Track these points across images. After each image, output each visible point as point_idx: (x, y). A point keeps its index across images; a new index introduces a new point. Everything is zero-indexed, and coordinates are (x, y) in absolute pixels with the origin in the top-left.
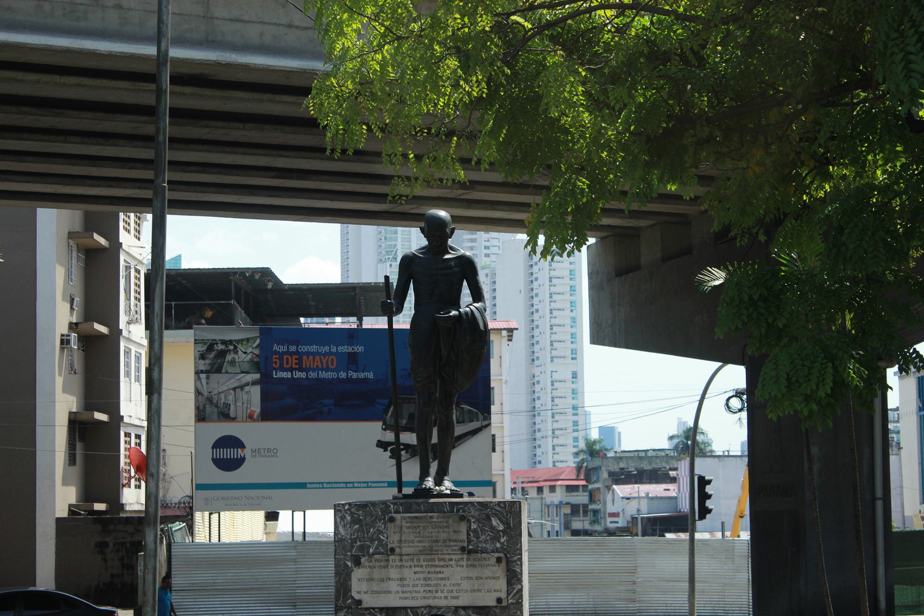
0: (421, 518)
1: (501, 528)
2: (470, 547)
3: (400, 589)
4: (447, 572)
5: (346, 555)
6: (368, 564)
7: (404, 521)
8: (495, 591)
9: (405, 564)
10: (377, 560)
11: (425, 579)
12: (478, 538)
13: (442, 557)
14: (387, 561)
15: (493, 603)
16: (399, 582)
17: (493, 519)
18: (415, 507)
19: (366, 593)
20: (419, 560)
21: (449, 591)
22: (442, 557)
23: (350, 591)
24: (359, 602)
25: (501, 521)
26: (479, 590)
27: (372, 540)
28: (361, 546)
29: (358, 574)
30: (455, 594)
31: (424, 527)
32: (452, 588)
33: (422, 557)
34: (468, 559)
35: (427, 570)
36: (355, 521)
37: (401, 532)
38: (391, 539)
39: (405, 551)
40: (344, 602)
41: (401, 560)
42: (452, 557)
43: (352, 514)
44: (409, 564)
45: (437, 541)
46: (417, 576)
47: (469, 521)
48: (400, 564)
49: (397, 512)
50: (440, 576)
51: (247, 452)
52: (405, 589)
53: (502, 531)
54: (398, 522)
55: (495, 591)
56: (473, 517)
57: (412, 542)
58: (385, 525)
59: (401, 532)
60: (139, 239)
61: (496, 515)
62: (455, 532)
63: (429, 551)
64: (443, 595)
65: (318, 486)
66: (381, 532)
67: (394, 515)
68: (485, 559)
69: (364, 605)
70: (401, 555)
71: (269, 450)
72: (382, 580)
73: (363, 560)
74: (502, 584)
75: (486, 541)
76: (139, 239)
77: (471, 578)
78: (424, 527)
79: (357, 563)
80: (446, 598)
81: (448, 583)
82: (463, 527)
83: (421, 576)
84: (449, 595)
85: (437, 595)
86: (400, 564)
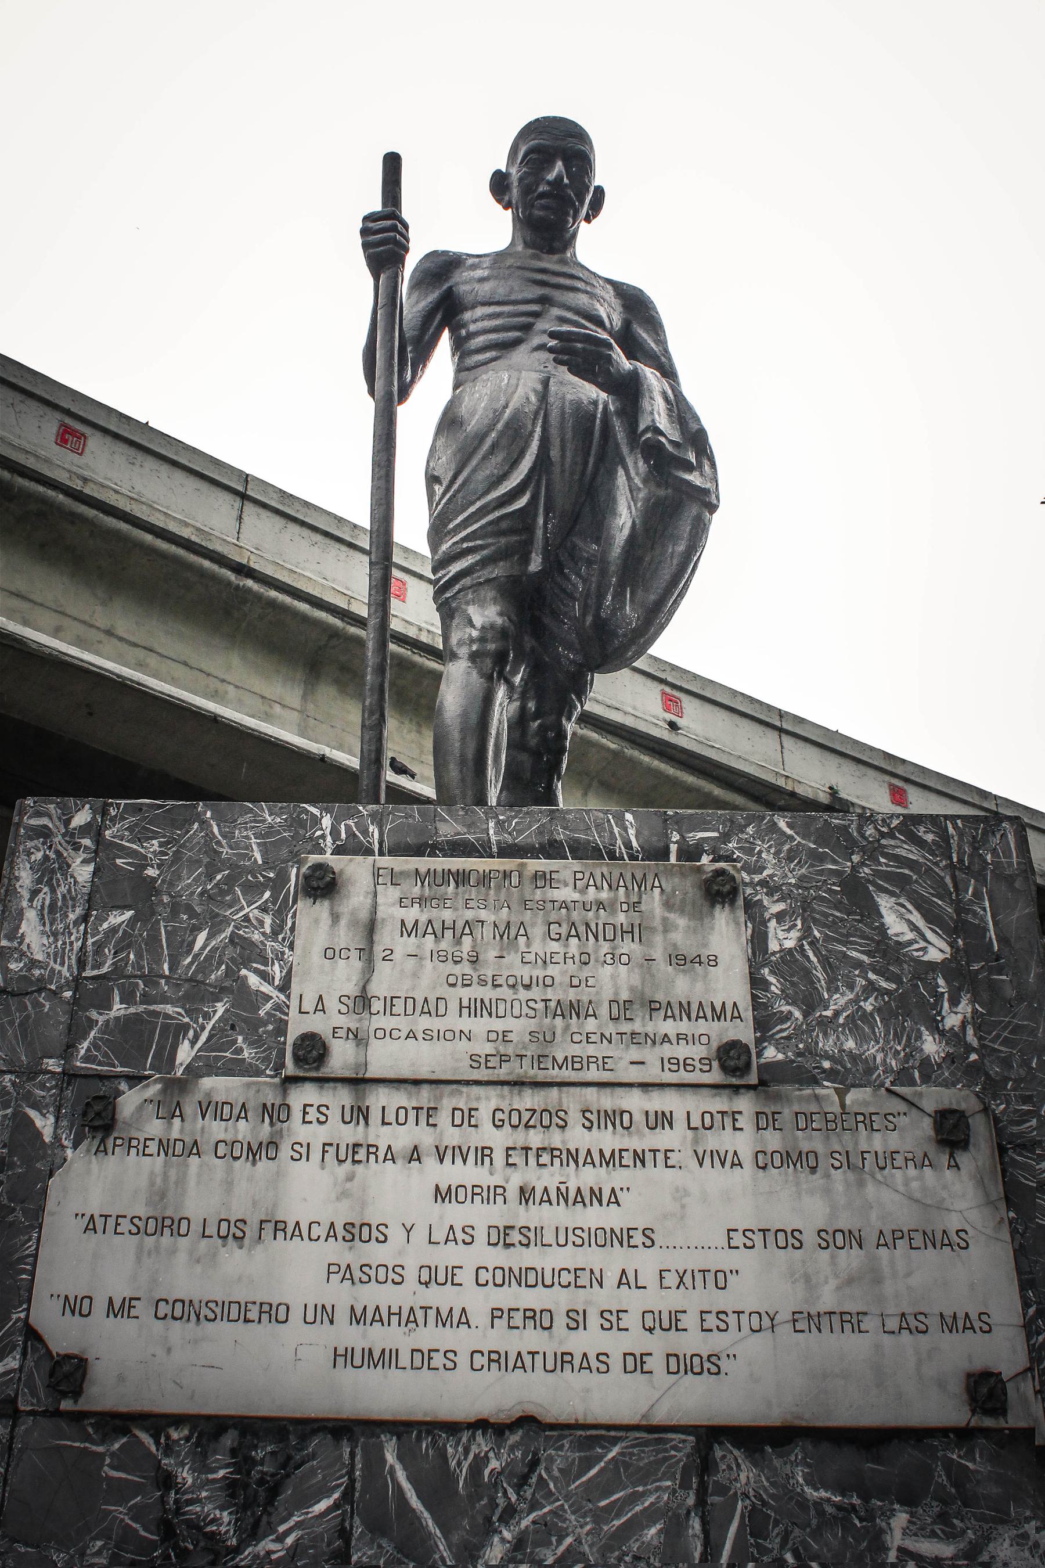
2: (771, 1053)
4: (643, 1196)
5: (33, 1072)
7: (389, 895)
9: (382, 1136)
11: (503, 1236)
12: (810, 1003)
13: (607, 1101)
14: (276, 1113)
15: (946, 1409)
17: (885, 903)
20: (468, 1118)
22: (607, 1101)
23: (26, 1295)
25: (931, 917)
27: (196, 994)
30: (692, 1342)
33: (488, 1101)
34: (764, 1121)
35: (516, 1180)
37: (367, 953)
38: (305, 989)
39: (383, 1058)
41: (360, 1114)
44: (402, 1137)
45: (574, 1009)
46: (457, 1214)
47: (752, 909)
48: (350, 1134)
50: (594, 1217)
52: (374, 1296)
54: (356, 900)
56: (771, 888)
57: (430, 1008)
59: (367, 953)
61: (900, 885)
62: (680, 960)
64: (615, 1344)
66: (248, 953)
72: (234, 1232)
73: (130, 1101)
75: (858, 1022)
77: (792, 1239)
78: (508, 935)
80: (637, 1363)
81: (645, 1263)
83: (482, 1216)
84: (658, 1344)
85: (579, 1343)
86: (350, 1134)
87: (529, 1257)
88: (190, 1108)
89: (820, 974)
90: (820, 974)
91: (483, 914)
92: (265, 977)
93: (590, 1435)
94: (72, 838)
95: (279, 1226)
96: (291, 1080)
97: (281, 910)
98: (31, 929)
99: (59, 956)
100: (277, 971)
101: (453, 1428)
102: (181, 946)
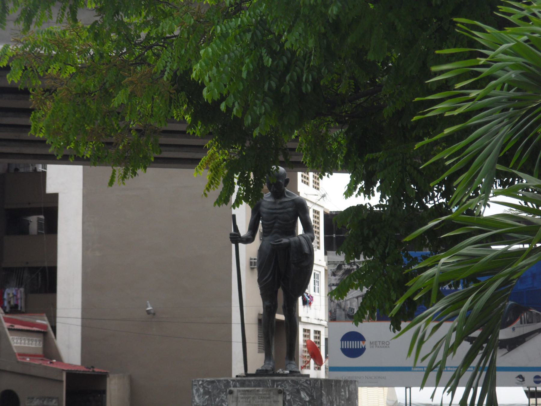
0: (251, 391)
1: (307, 399)
7: (239, 393)
17: (302, 393)
18: (247, 383)
25: (307, 394)
31: (253, 398)
36: (206, 393)
43: (204, 388)
47: (284, 394)
49: (235, 386)
51: (367, 344)
53: (309, 402)
54: (235, 394)
56: (287, 390)
58: (227, 395)
60: (318, 189)
61: (304, 390)
65: (420, 369)
67: (232, 388)
71: (383, 343)
76: (318, 189)
78: (253, 398)
82: (280, 398)
89: (292, 403)
90: (292, 403)
94: (200, 385)
97: (227, 395)
99: (200, 402)
102: (215, 400)
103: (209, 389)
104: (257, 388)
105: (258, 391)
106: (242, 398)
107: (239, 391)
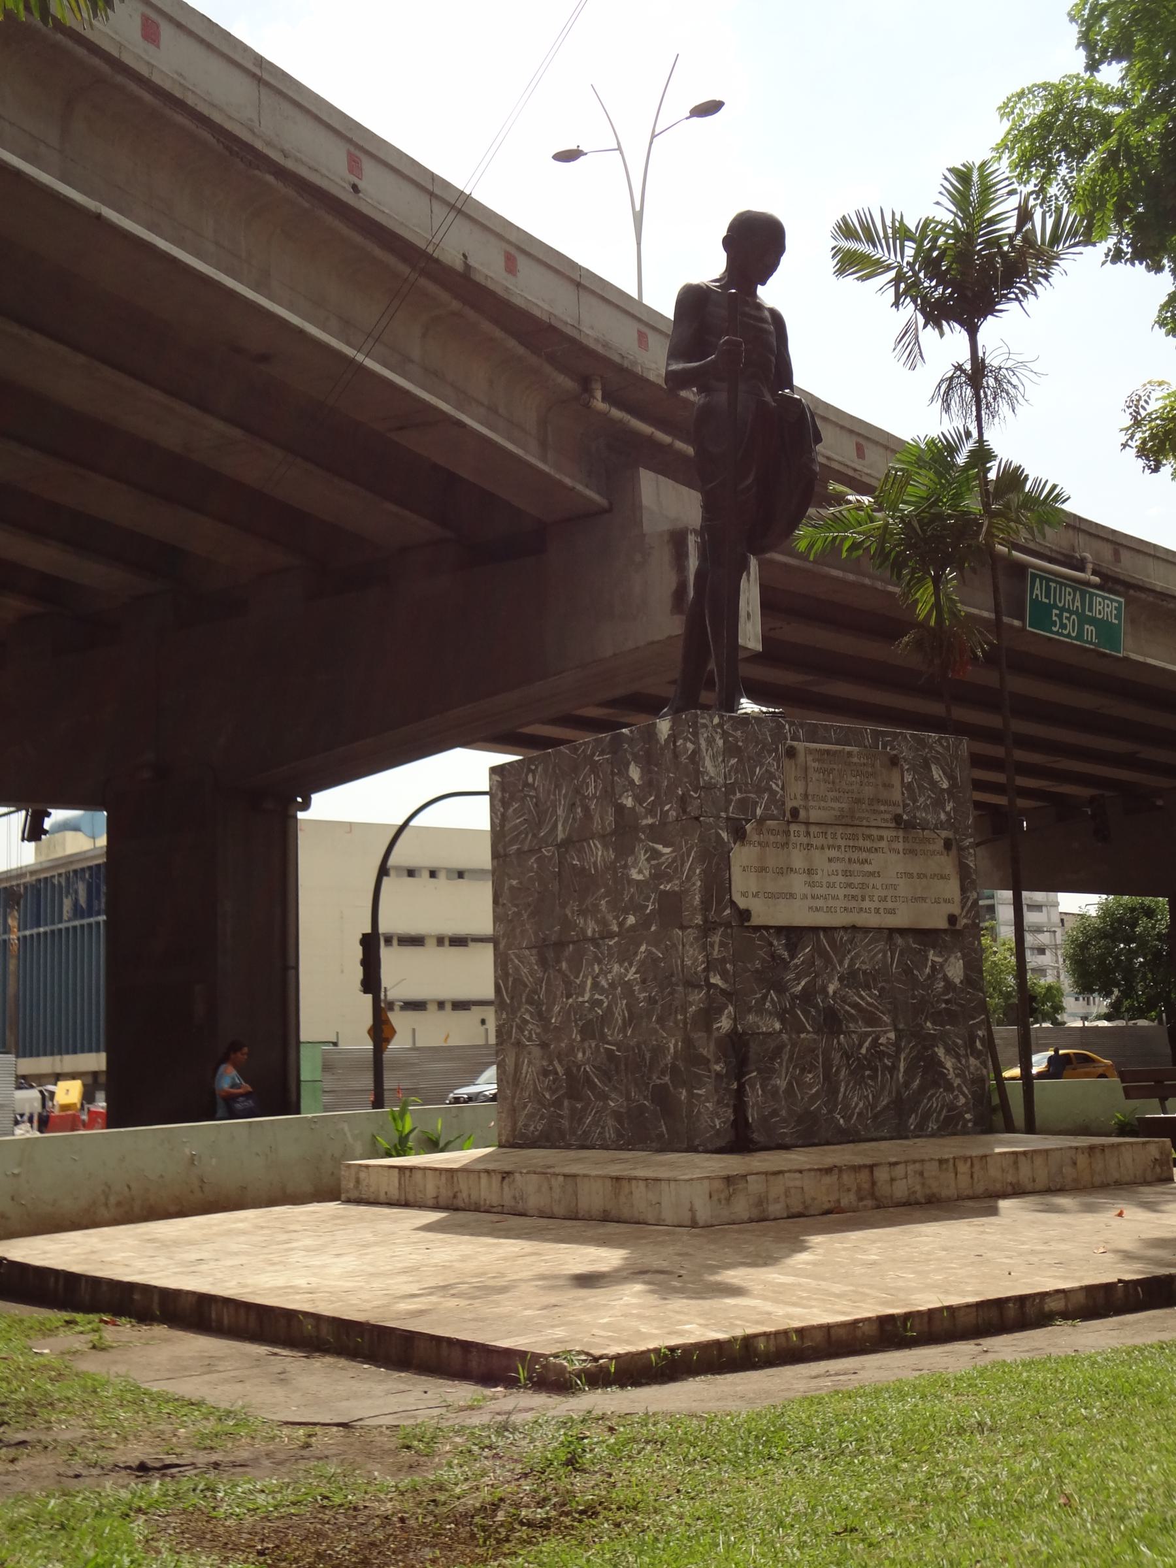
3: (807, 890)
5: (718, 817)
6: (755, 838)
7: (810, 758)
8: (945, 901)
9: (814, 842)
10: (771, 831)
11: (846, 873)
12: (915, 801)
15: (942, 924)
16: (804, 877)
17: (933, 767)
19: (756, 895)
20: (834, 836)
21: (884, 899)
22: (868, 832)
24: (745, 915)
26: (923, 899)
27: (759, 791)
28: (741, 801)
29: (742, 857)
30: (890, 905)
32: (883, 893)
34: (905, 839)
36: (731, 750)
39: (815, 815)
40: (719, 911)
42: (886, 834)
43: (725, 735)
44: (820, 841)
48: (805, 840)
50: (867, 868)
52: (818, 891)
55: (945, 901)
61: (937, 761)
63: (847, 821)
64: (873, 905)
68: (928, 840)
69: (755, 921)
70: (807, 824)
74: (951, 888)
75: (926, 808)
77: (911, 876)
79: (739, 835)
80: (877, 911)
81: (877, 881)
83: (838, 866)
84: (882, 905)
86: (805, 840)
87: (851, 880)
88: (764, 831)
91: (835, 766)
92: (777, 785)
93: (866, 930)
94: (713, 727)
95: (792, 870)
96: (789, 822)
98: (708, 763)
99: (718, 774)
100: (780, 783)
101: (835, 928)
103: (736, 739)
104: (848, 748)
105: (850, 754)
106: (816, 770)
107: (809, 751)
